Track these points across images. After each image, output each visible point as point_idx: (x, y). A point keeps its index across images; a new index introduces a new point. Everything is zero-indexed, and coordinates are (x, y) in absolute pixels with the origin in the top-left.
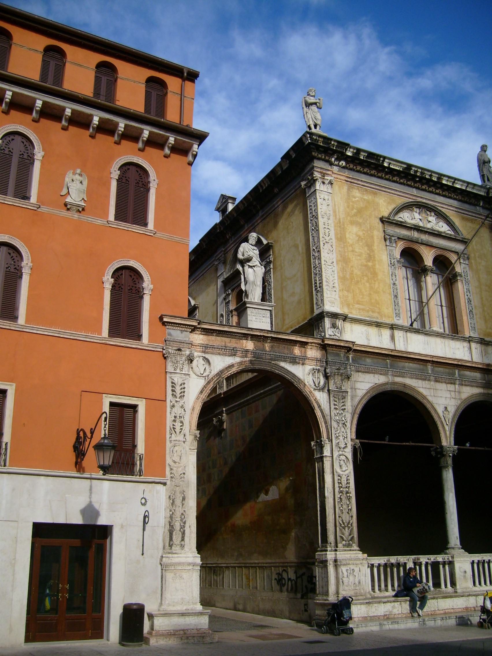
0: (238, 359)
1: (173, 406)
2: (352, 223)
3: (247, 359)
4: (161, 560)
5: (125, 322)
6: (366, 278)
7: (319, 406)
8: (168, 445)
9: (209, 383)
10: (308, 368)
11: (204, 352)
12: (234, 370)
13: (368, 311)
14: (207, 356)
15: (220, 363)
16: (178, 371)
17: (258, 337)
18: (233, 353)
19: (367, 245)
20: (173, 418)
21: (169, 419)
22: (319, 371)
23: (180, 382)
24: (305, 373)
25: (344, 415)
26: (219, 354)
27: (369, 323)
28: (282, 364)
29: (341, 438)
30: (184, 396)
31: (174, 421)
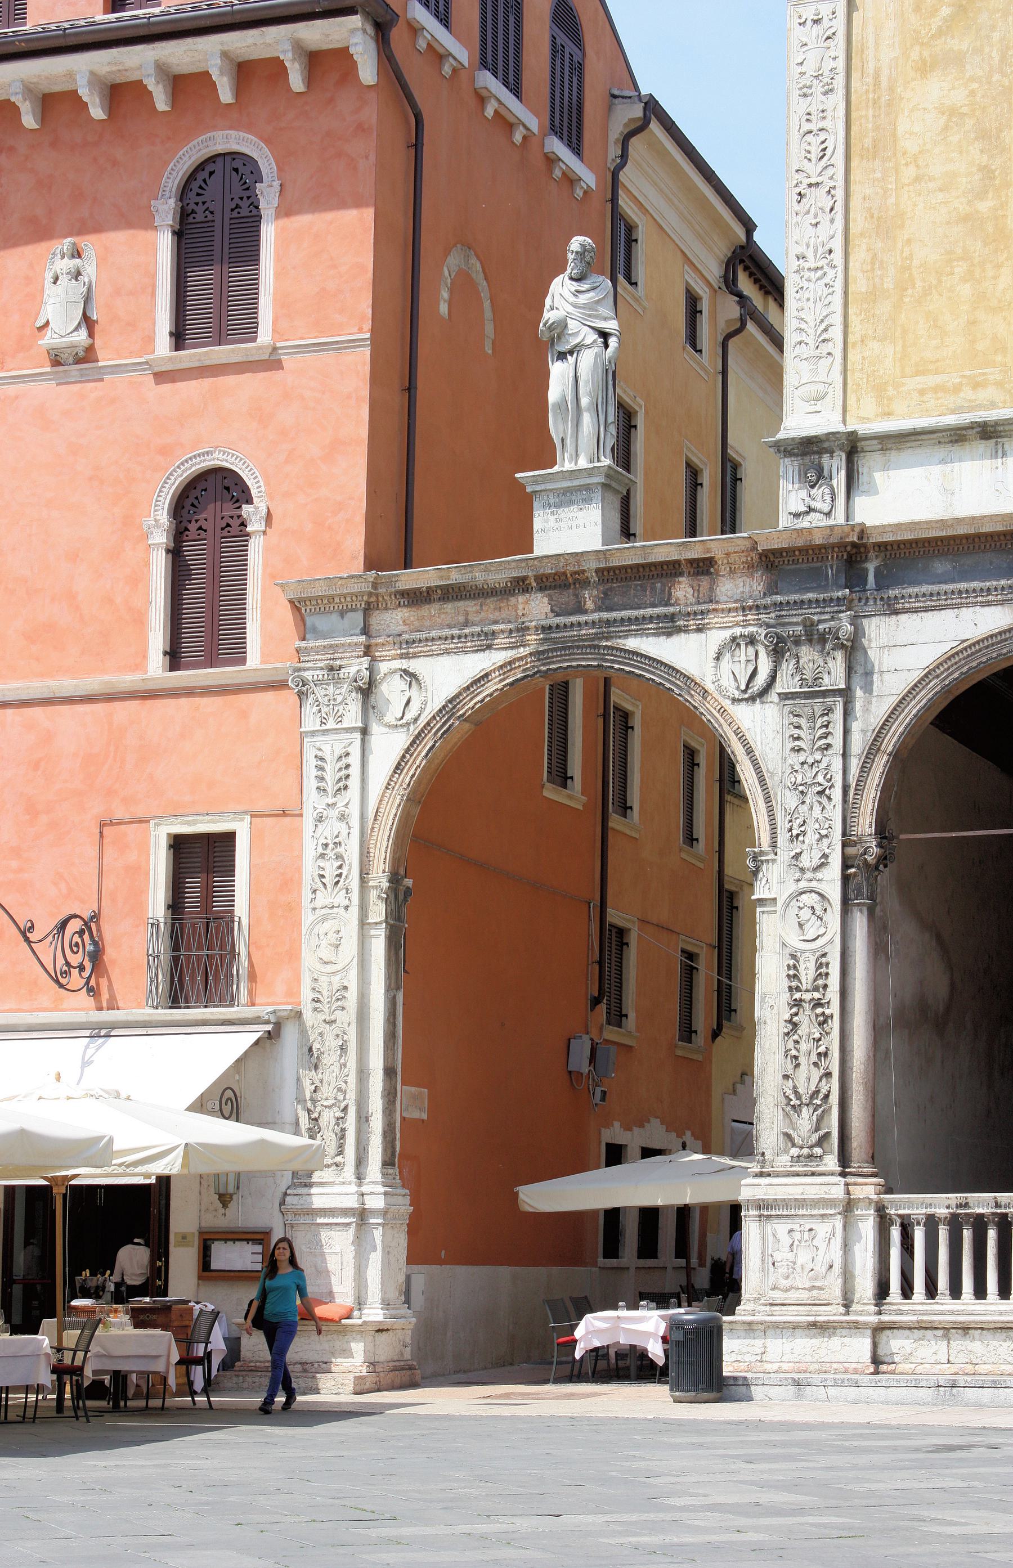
0: (498, 657)
1: (320, 819)
2: (924, 69)
3: (522, 651)
4: (283, 1203)
5: (201, 621)
6: (960, 269)
7: (749, 751)
8: (308, 918)
9: (418, 738)
10: (717, 637)
11: (407, 656)
12: (492, 687)
13: (957, 389)
14: (413, 665)
15: (450, 674)
16: (331, 724)
17: (561, 580)
18: (486, 642)
19: (983, 135)
20: (320, 850)
21: (310, 850)
22: (752, 641)
23: (339, 750)
24: (703, 657)
25: (823, 765)
26: (447, 652)
27: (956, 437)
28: (632, 643)
29: (811, 838)
30: (346, 787)
31: (322, 856)
